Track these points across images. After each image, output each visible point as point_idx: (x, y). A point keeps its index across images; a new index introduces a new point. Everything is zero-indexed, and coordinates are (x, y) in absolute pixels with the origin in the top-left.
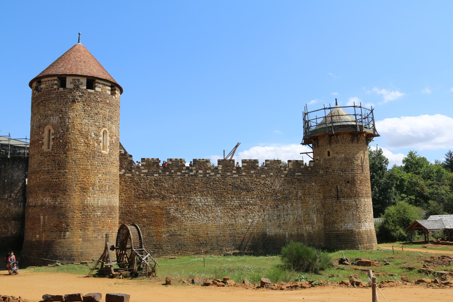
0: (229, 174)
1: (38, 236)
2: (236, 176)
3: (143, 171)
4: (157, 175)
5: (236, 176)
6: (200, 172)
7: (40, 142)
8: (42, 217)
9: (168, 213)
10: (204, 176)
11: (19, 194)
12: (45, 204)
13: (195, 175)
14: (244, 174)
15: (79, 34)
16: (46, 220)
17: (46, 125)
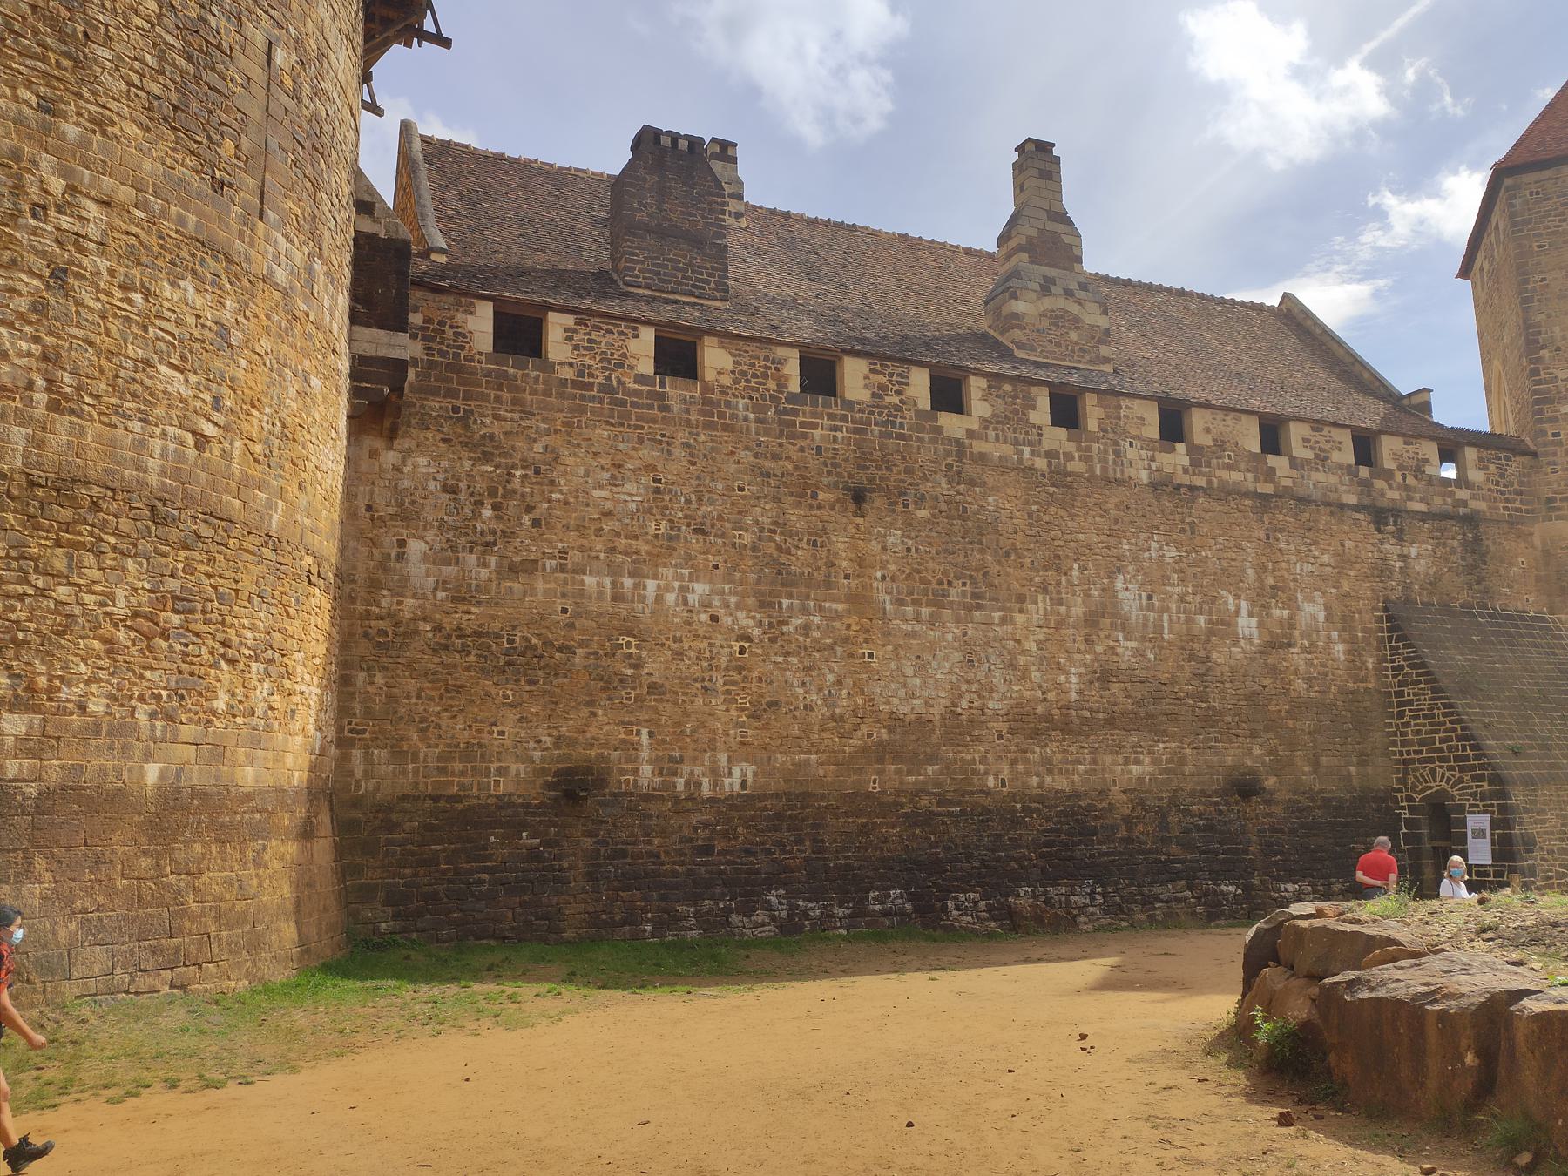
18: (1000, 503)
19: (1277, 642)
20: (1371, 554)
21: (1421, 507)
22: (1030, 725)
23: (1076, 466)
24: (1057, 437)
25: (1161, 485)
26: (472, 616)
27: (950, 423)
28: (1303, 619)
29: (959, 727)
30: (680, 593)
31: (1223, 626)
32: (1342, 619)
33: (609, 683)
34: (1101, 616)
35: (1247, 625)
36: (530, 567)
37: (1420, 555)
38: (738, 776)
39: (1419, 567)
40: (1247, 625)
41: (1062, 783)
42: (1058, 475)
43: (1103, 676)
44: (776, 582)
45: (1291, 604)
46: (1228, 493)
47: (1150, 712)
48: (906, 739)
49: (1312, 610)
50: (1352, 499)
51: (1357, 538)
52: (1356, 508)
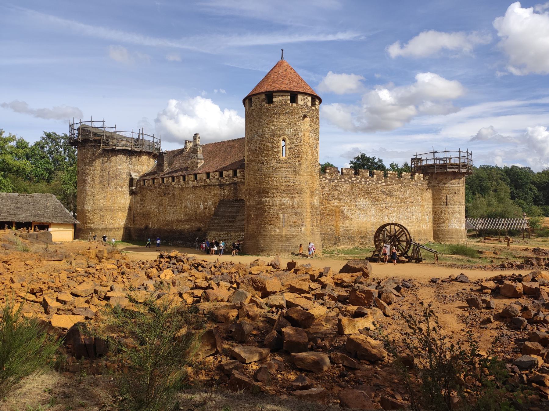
0: (380, 182)
1: (278, 230)
2: (384, 184)
3: (328, 177)
4: (336, 181)
5: (384, 184)
6: (363, 180)
7: (275, 150)
8: (281, 215)
9: (343, 212)
10: (366, 183)
11: (124, 187)
12: (284, 204)
13: (360, 183)
14: (389, 183)
15: (282, 50)
16: (285, 217)
17: (281, 135)
18: (177, 193)
19: (205, 208)
20: (219, 192)
21: (228, 183)
22: (179, 221)
23: (184, 186)
24: (182, 183)
25: (194, 187)
26: (141, 211)
27: (173, 184)
28: (209, 204)
29: (172, 221)
30: (153, 208)
31: (199, 207)
32: (214, 204)
33: (149, 217)
34: (186, 207)
35: (202, 206)
36: (144, 207)
37: (226, 191)
38: (156, 227)
39: (226, 194)
40: (202, 206)
41: (181, 228)
42: (182, 187)
43: (185, 215)
44: (159, 205)
45: (207, 202)
46: (201, 186)
47: (190, 219)
48: (168, 223)
49: (210, 203)
50: (217, 184)
51: (217, 190)
52: (217, 185)
